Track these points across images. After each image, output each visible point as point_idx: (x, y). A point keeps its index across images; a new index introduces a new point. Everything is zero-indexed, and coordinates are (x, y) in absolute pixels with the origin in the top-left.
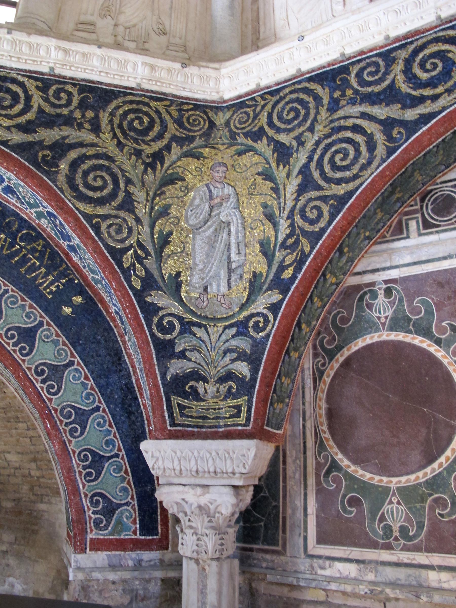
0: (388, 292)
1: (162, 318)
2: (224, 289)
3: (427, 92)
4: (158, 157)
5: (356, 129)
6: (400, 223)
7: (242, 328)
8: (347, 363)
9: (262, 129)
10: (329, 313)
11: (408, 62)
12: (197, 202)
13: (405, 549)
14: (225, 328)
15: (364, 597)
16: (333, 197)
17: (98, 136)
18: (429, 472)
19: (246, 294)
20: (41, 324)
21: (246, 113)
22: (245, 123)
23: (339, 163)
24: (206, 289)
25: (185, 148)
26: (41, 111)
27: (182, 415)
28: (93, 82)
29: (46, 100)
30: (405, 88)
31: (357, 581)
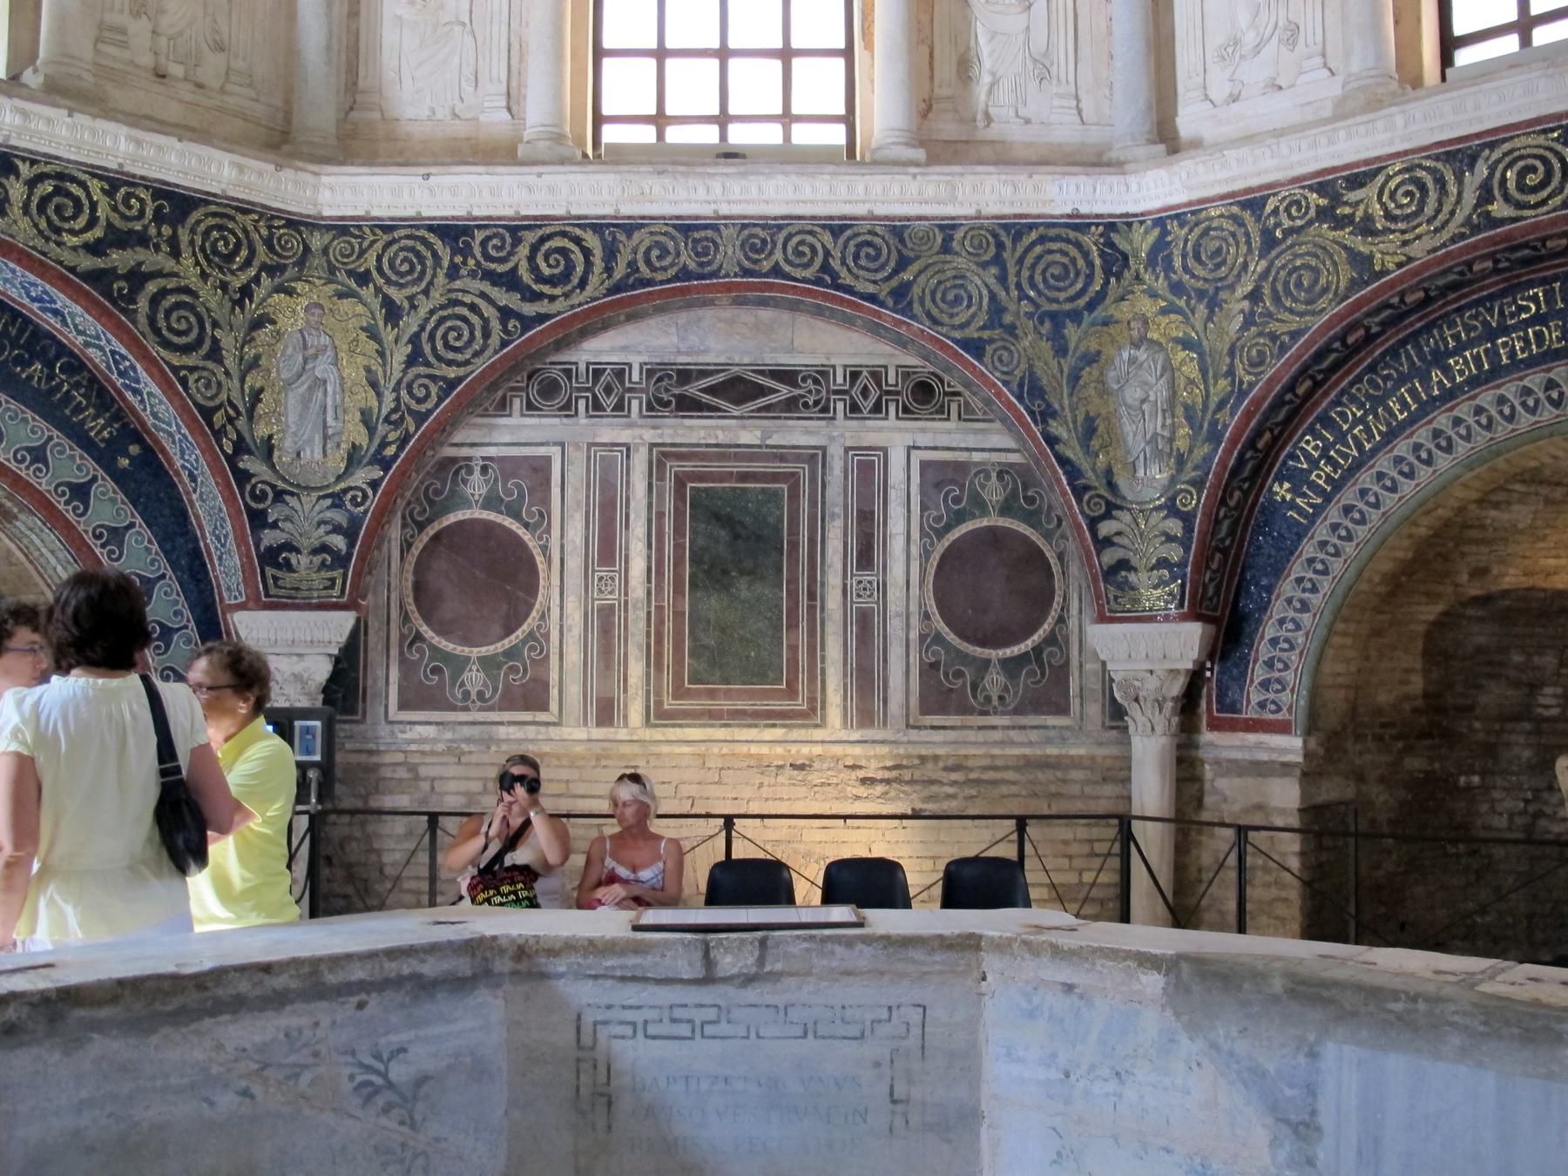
0: (484, 469)
1: (254, 486)
2: (318, 455)
3: (546, 289)
4: (246, 291)
5: (473, 308)
6: (504, 398)
7: (337, 500)
8: (436, 538)
9: (368, 272)
10: (422, 482)
11: (534, 249)
12: (289, 351)
13: (481, 709)
14: (320, 498)
15: (441, 754)
16: (443, 378)
17: (178, 262)
18: (507, 643)
19: (343, 465)
20: (94, 479)
21: (349, 243)
22: (348, 256)
23: (452, 343)
24: (298, 454)
25: (277, 280)
26: (110, 225)
27: (277, 586)
28: (168, 184)
29: (115, 209)
30: (525, 276)
31: (435, 741)
